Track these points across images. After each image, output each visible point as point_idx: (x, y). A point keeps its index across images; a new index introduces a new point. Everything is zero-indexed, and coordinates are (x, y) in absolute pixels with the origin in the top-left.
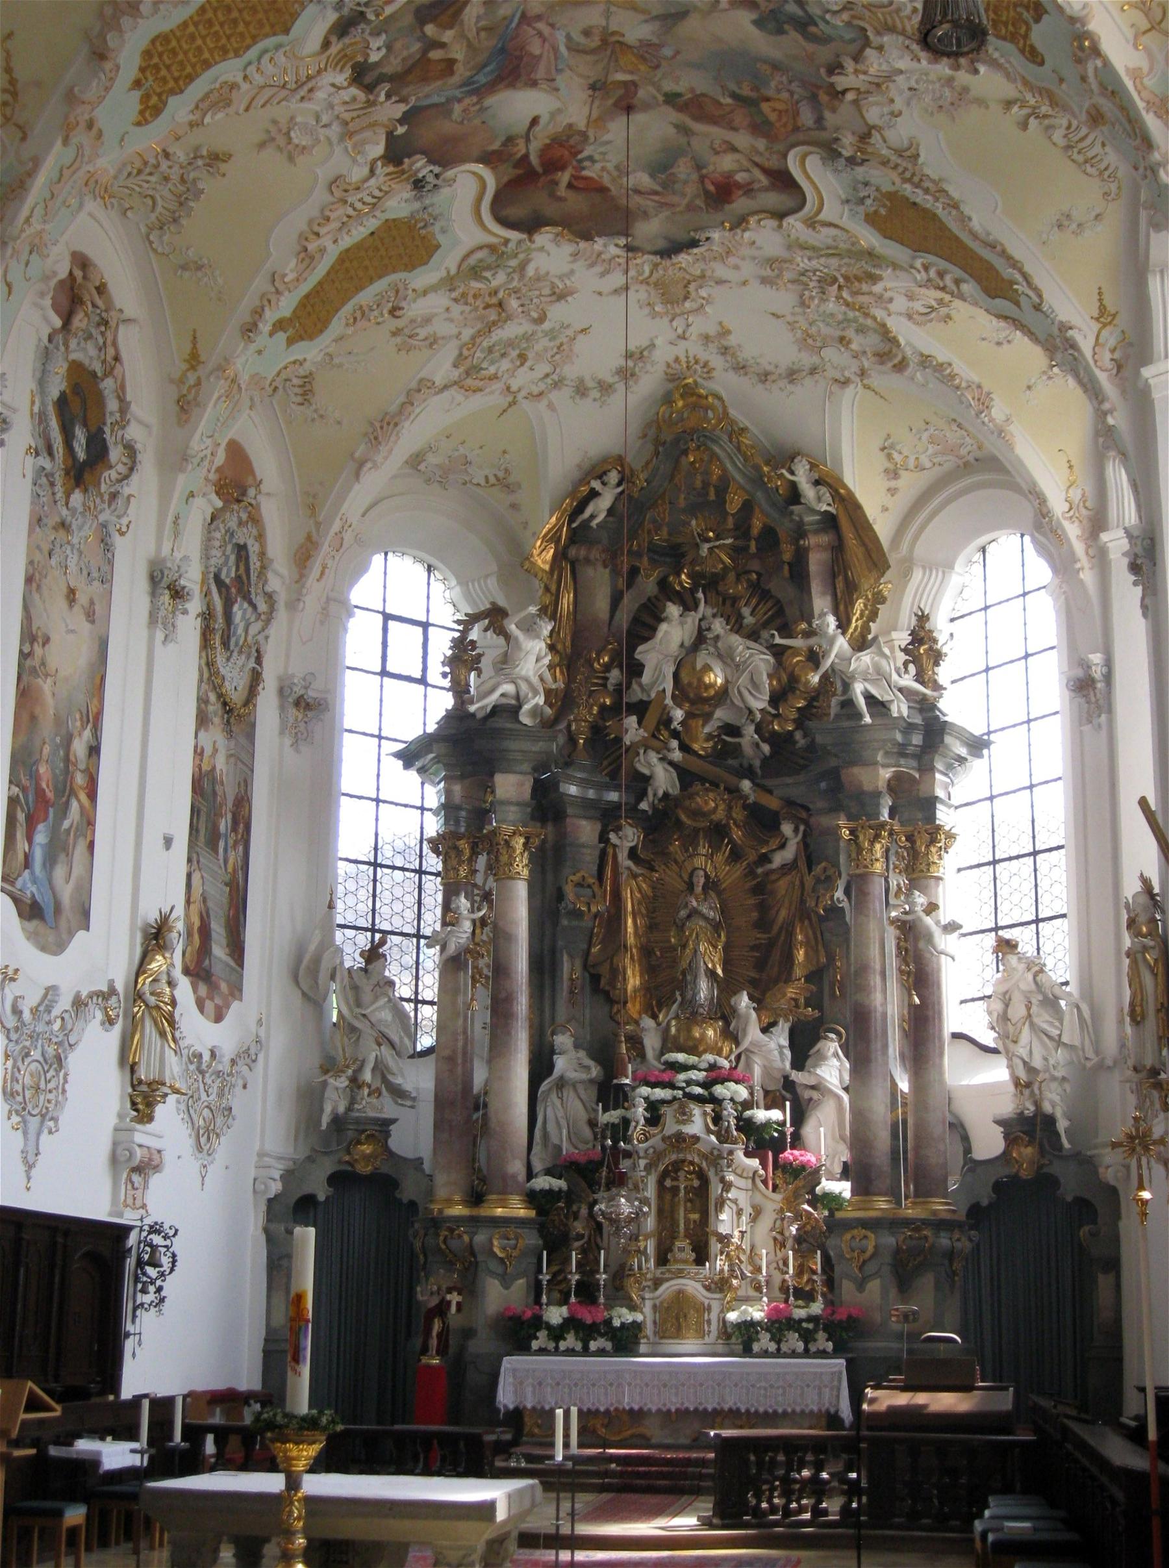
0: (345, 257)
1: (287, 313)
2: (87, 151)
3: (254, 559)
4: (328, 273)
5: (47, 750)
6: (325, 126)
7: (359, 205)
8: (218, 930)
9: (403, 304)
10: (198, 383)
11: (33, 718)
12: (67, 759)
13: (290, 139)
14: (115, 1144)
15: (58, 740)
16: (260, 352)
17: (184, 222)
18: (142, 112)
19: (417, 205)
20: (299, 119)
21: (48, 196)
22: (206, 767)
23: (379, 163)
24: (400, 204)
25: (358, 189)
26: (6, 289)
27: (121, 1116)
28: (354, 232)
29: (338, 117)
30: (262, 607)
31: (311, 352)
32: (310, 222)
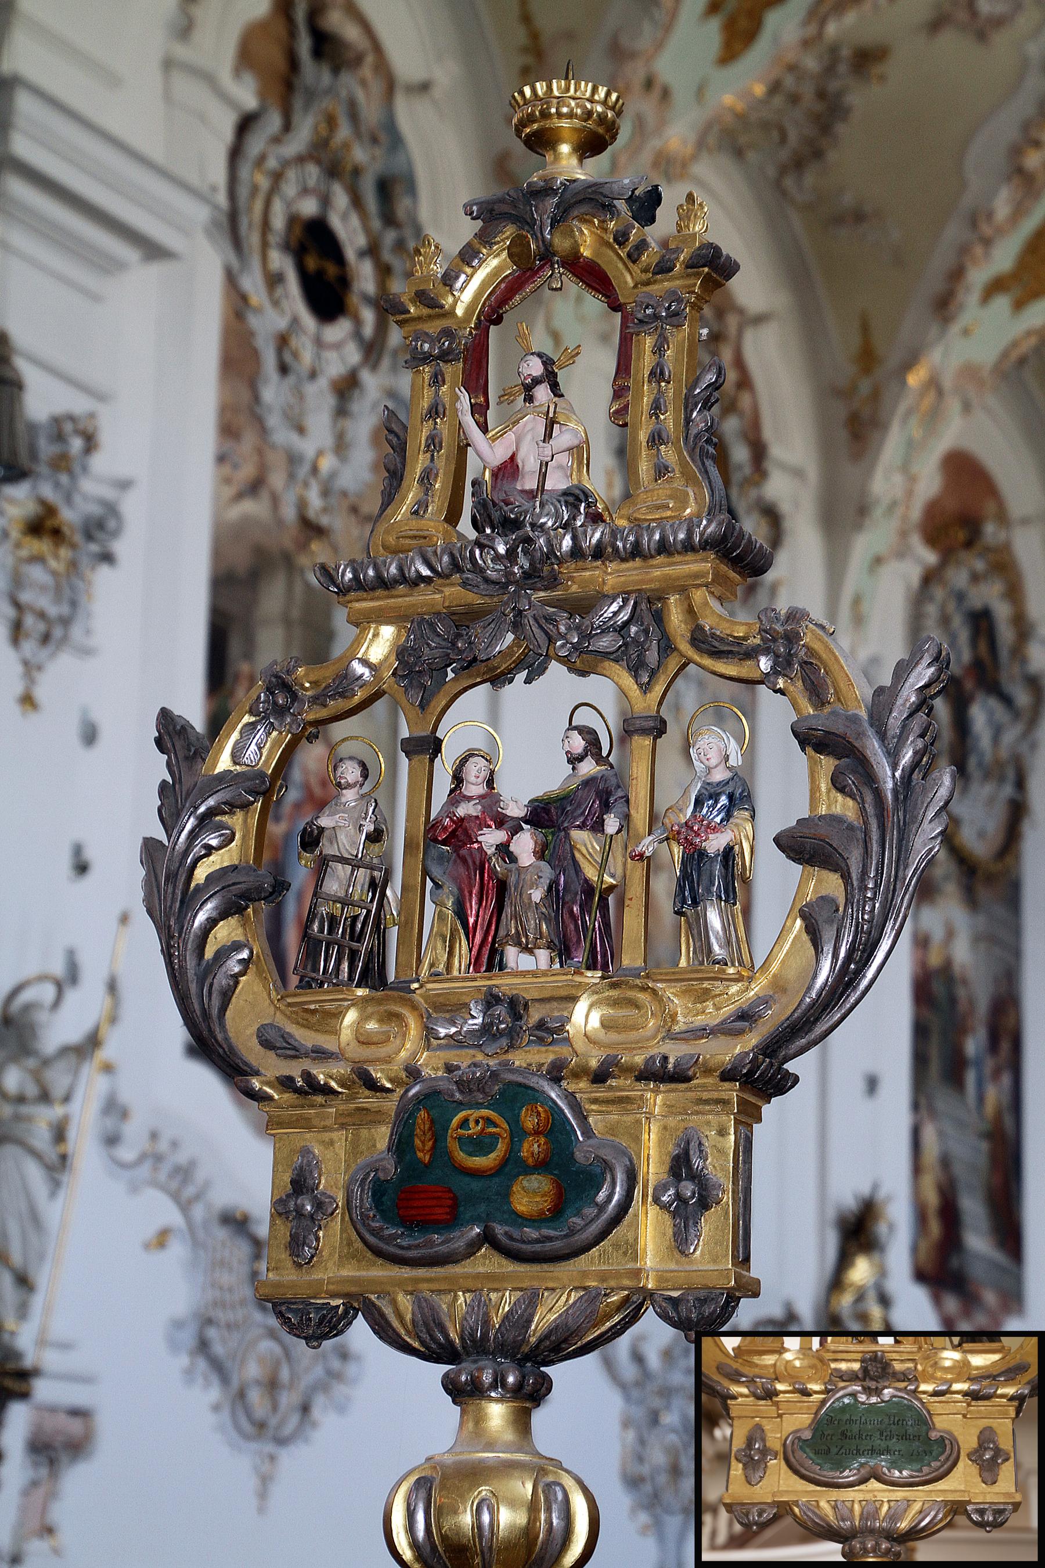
3: (1006, 634)
8: (973, 1208)
10: (875, 396)
22: (935, 960)
30: (1022, 698)
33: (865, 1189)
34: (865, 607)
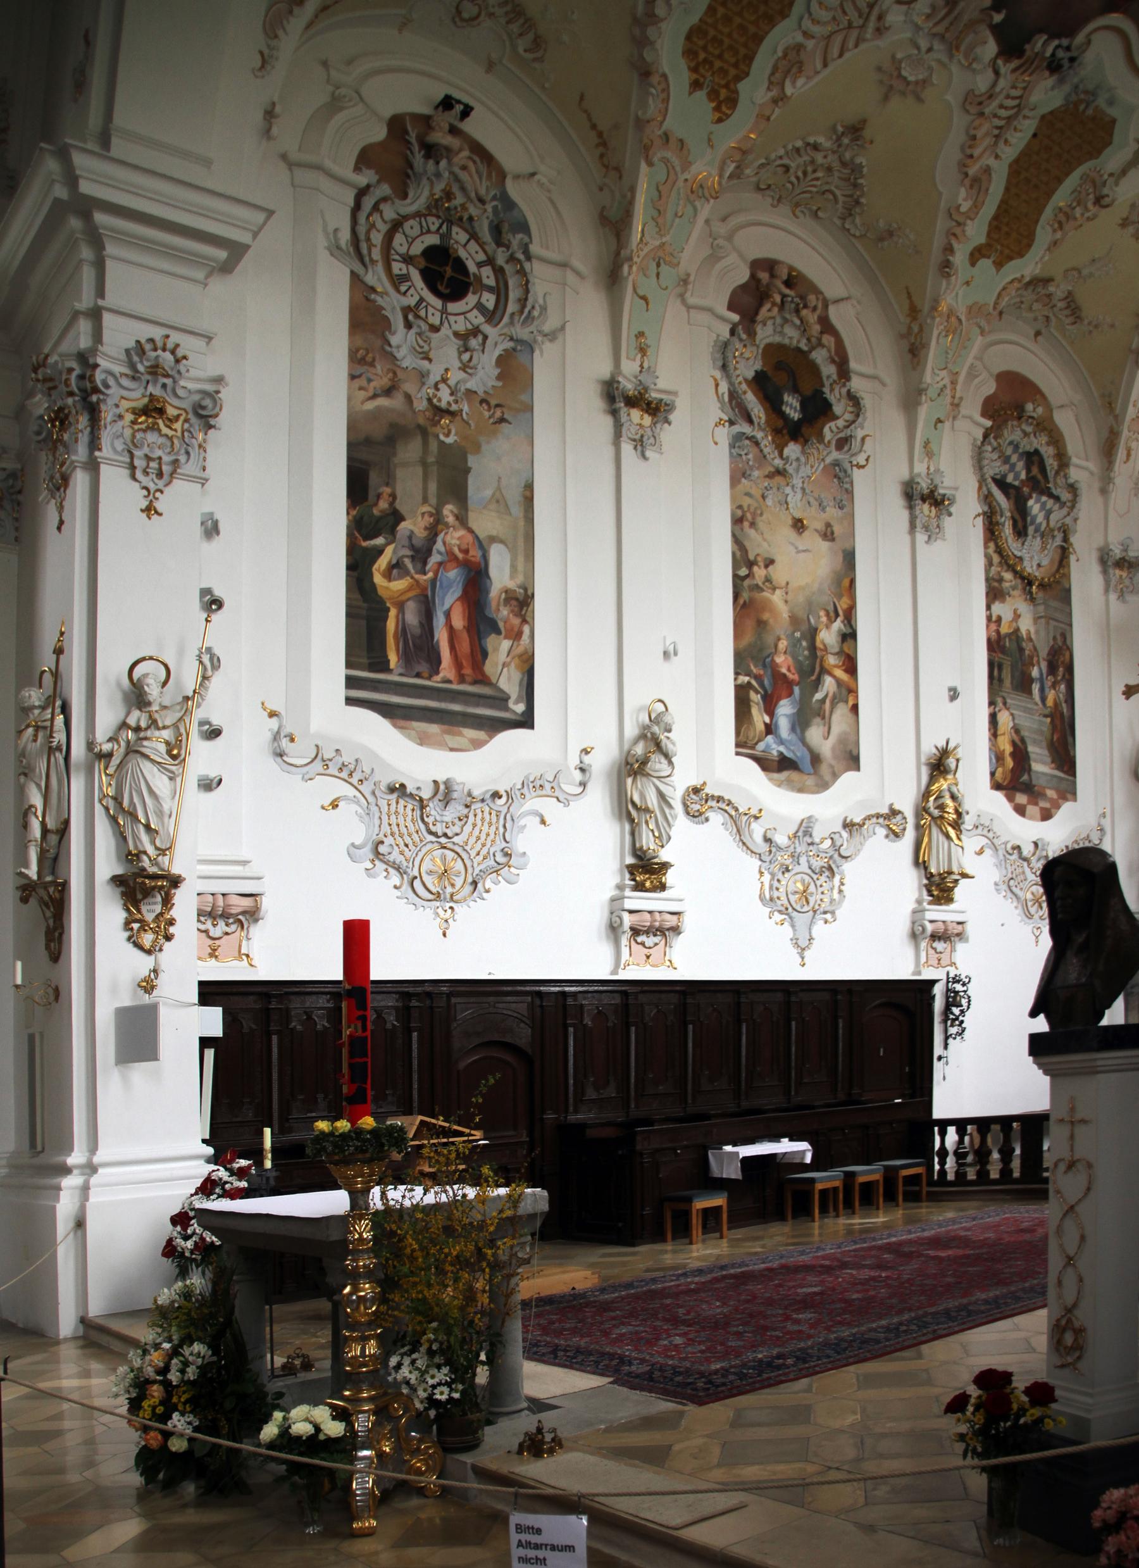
0: (1016, 168)
1: (982, 239)
2: (676, 162)
4: (1007, 189)
5: (783, 644)
6: (930, 50)
7: (1003, 113)
9: (1105, 191)
10: (921, 330)
11: (761, 624)
12: (813, 647)
13: (905, 78)
14: (913, 923)
15: (798, 634)
16: (967, 283)
17: (863, 200)
18: (717, 109)
19: (1067, 88)
20: (899, 56)
21: (656, 214)
23: (1000, 62)
24: (1046, 95)
25: (990, 97)
26: (642, 302)
27: (919, 902)
28: (1013, 141)
29: (935, 35)
31: (1027, 266)
32: (962, 149)
33: (941, 744)
34: (933, 446)
